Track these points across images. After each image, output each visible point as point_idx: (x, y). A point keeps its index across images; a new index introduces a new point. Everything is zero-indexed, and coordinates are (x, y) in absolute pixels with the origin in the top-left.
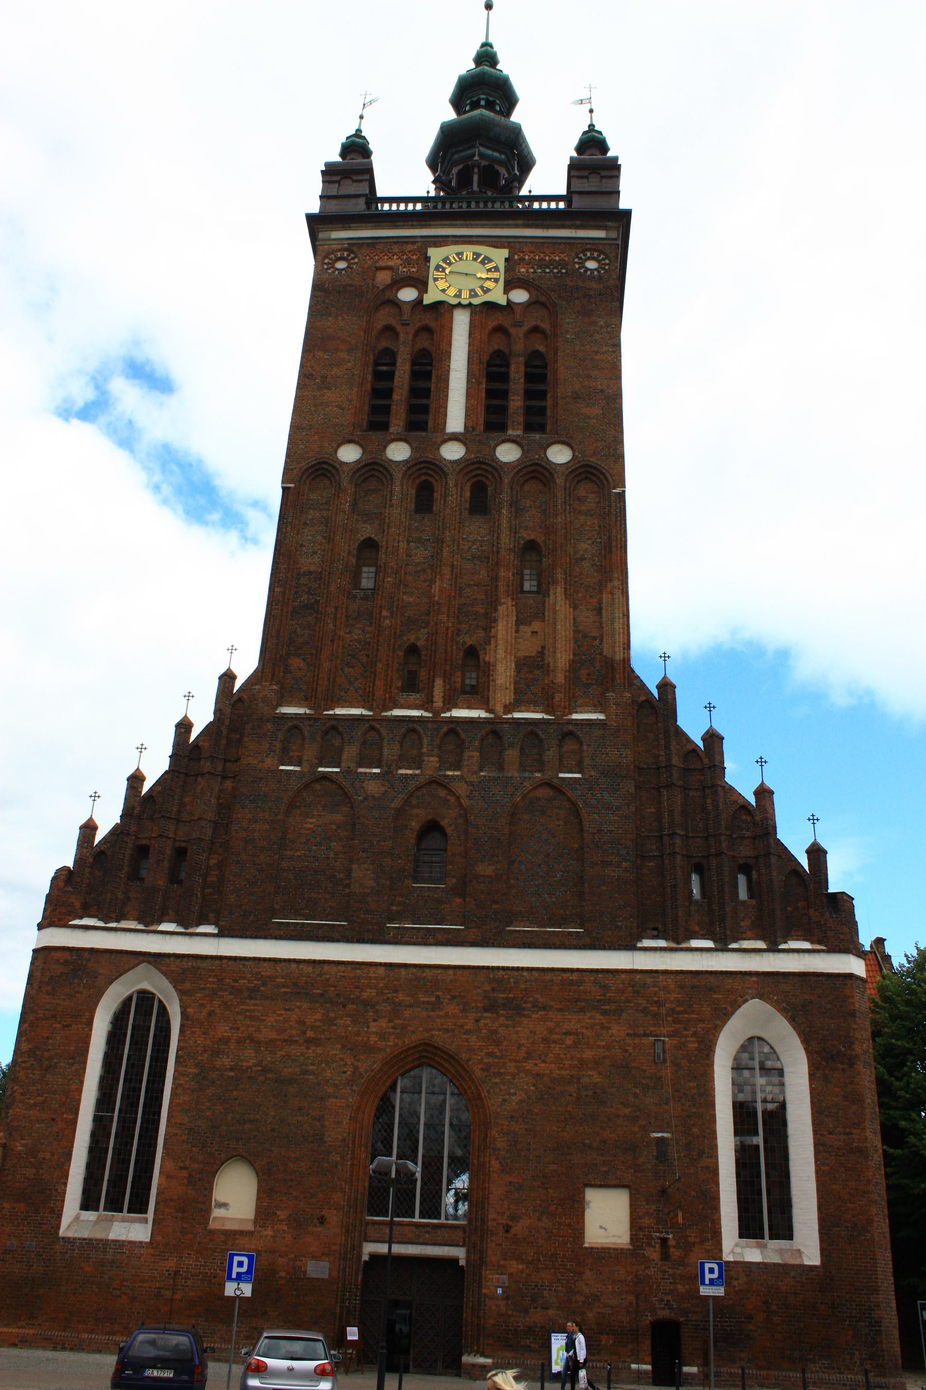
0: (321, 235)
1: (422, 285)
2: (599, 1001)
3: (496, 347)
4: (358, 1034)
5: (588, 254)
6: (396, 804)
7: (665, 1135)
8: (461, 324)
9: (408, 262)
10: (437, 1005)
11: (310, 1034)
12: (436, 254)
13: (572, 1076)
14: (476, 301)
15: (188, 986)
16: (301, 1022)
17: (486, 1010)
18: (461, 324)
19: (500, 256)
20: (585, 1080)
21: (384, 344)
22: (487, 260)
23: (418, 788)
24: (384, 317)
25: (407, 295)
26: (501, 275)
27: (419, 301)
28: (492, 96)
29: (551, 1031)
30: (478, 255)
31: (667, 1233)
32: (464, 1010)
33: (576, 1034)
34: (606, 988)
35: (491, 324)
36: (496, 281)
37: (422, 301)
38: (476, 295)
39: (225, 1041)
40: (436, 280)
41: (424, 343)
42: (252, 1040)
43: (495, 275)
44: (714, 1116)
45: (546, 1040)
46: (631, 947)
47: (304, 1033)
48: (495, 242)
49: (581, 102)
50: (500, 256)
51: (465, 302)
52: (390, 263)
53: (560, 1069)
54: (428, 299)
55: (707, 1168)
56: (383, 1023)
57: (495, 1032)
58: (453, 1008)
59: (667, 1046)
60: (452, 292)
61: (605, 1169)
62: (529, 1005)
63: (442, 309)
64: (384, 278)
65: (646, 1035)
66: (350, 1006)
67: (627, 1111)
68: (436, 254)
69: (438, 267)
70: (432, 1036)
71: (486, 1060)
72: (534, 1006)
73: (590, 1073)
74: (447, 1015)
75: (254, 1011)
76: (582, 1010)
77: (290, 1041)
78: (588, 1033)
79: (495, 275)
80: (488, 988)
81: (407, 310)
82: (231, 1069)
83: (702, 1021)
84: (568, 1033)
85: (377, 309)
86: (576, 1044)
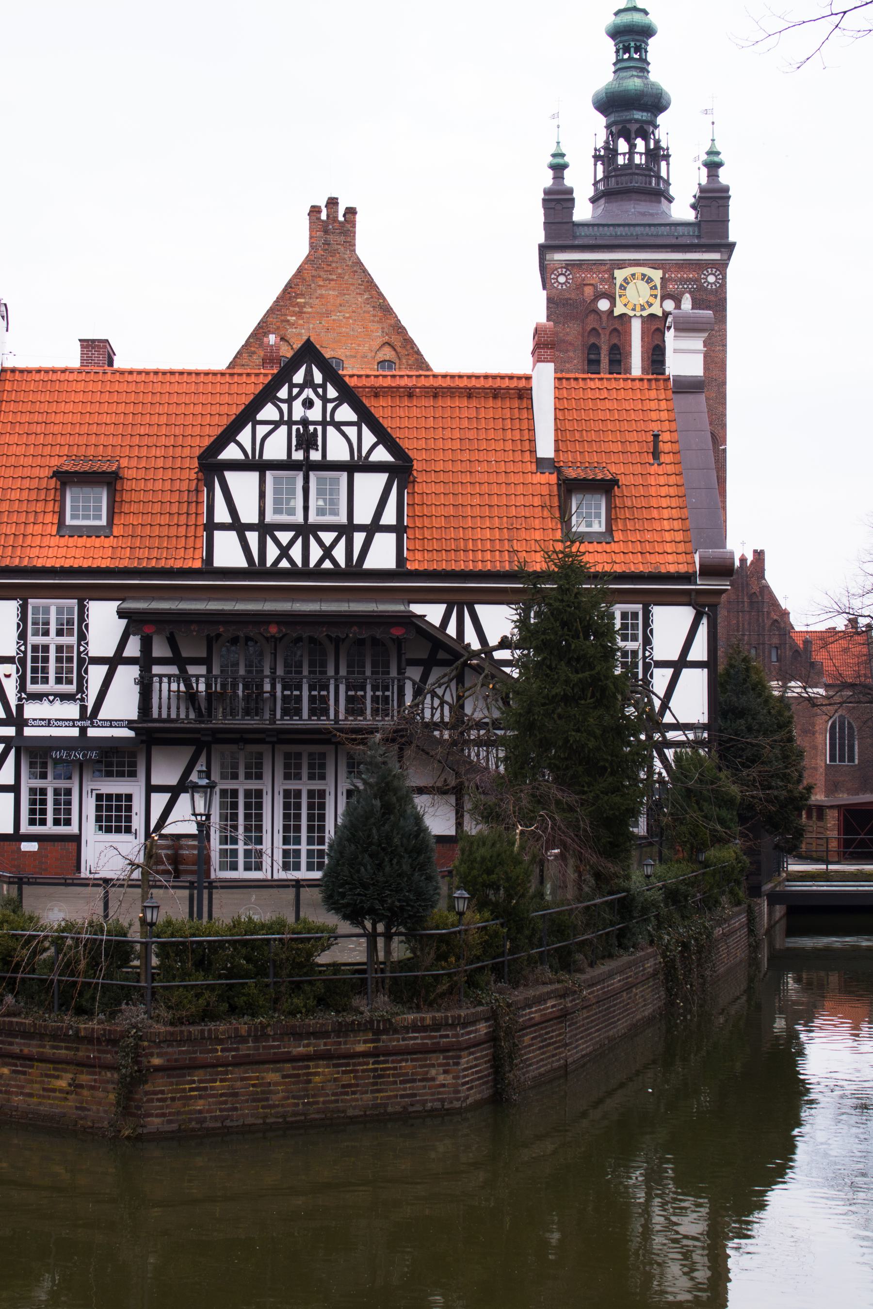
0: (548, 257)
1: (612, 299)
3: (656, 342)
5: (709, 270)
8: (636, 327)
9: (602, 280)
12: (620, 275)
14: (645, 313)
18: (636, 327)
19: (656, 275)
21: (593, 340)
22: (649, 280)
24: (591, 322)
25: (603, 305)
26: (658, 292)
27: (611, 311)
28: (638, 41)
30: (644, 275)
35: (654, 328)
36: (656, 297)
37: (612, 312)
38: (643, 308)
40: (620, 296)
41: (615, 341)
43: (655, 292)
49: (706, 112)
50: (656, 275)
51: (638, 314)
52: (592, 282)
54: (617, 312)
60: (630, 306)
64: (588, 291)
68: (620, 275)
69: (621, 286)
79: (655, 292)
81: (604, 318)
85: (587, 316)
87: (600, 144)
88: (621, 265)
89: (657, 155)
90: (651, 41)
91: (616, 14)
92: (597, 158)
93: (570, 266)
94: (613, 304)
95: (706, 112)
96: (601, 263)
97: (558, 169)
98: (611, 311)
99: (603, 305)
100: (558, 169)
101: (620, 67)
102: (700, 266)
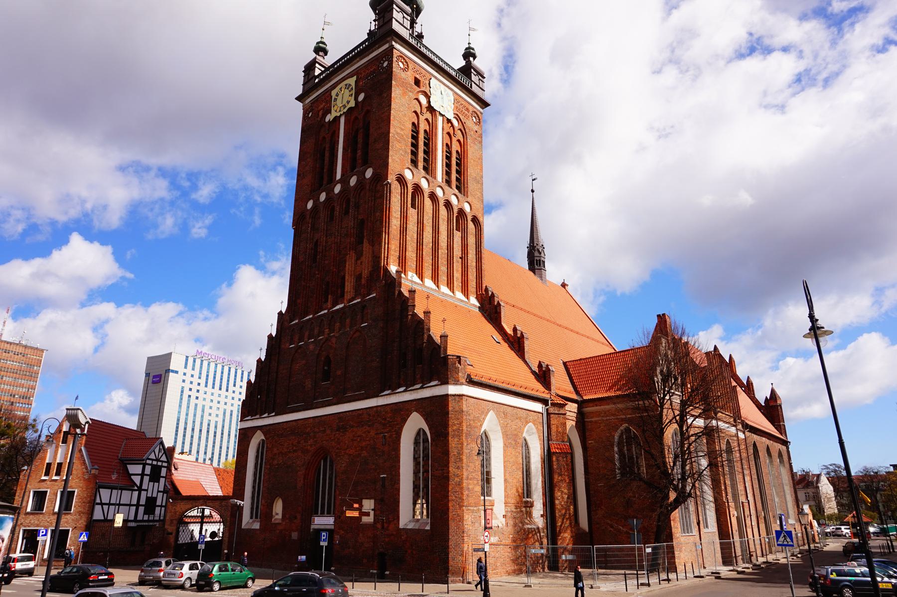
2: (367, 421)
4: (305, 446)
6: (317, 353)
7: (385, 476)
10: (324, 431)
11: (294, 448)
13: (359, 454)
14: (345, 110)
15: (268, 436)
16: (292, 444)
17: (337, 430)
20: (362, 455)
23: (324, 343)
29: (354, 436)
31: (384, 517)
32: (331, 432)
33: (361, 436)
34: (369, 415)
39: (275, 454)
42: (281, 452)
44: (399, 466)
45: (352, 440)
46: (377, 396)
47: (293, 448)
53: (356, 451)
55: (397, 488)
56: (311, 441)
57: (339, 439)
58: (328, 432)
59: (387, 437)
61: (367, 491)
62: (348, 426)
65: (381, 433)
66: (304, 436)
67: (374, 466)
70: (323, 444)
71: (336, 451)
72: (350, 427)
73: (364, 452)
74: (327, 435)
75: (281, 442)
76: (363, 426)
77: (290, 452)
78: (364, 435)
80: (337, 421)
82: (277, 465)
83: (398, 424)
84: (359, 436)
86: (361, 440)
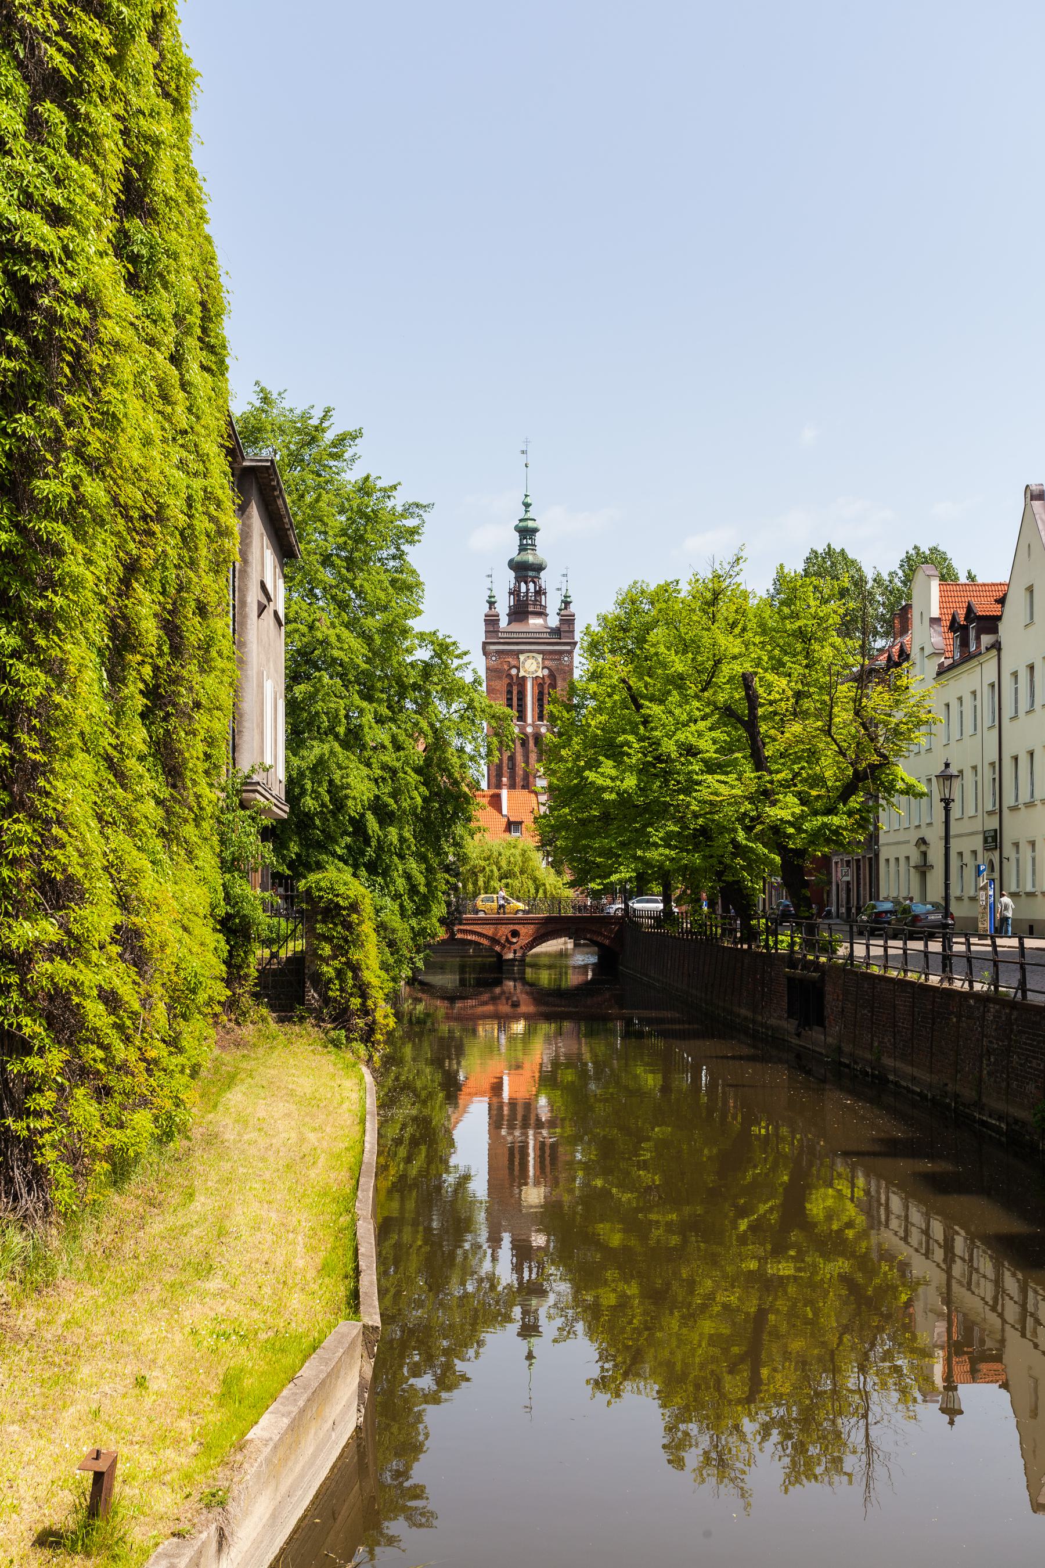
1: (518, 669)
12: (522, 657)
48: (539, 652)
49: (564, 575)
50: (540, 657)
54: (521, 675)
63: (524, 678)
68: (522, 657)
87: (512, 586)
88: (522, 652)
89: (540, 592)
90: (537, 534)
91: (521, 520)
92: (510, 593)
93: (498, 652)
94: (519, 671)
95: (564, 575)
96: (513, 651)
97: (491, 604)
98: (518, 675)
99: (514, 672)
100: (491, 604)
101: (522, 548)
102: (561, 652)
